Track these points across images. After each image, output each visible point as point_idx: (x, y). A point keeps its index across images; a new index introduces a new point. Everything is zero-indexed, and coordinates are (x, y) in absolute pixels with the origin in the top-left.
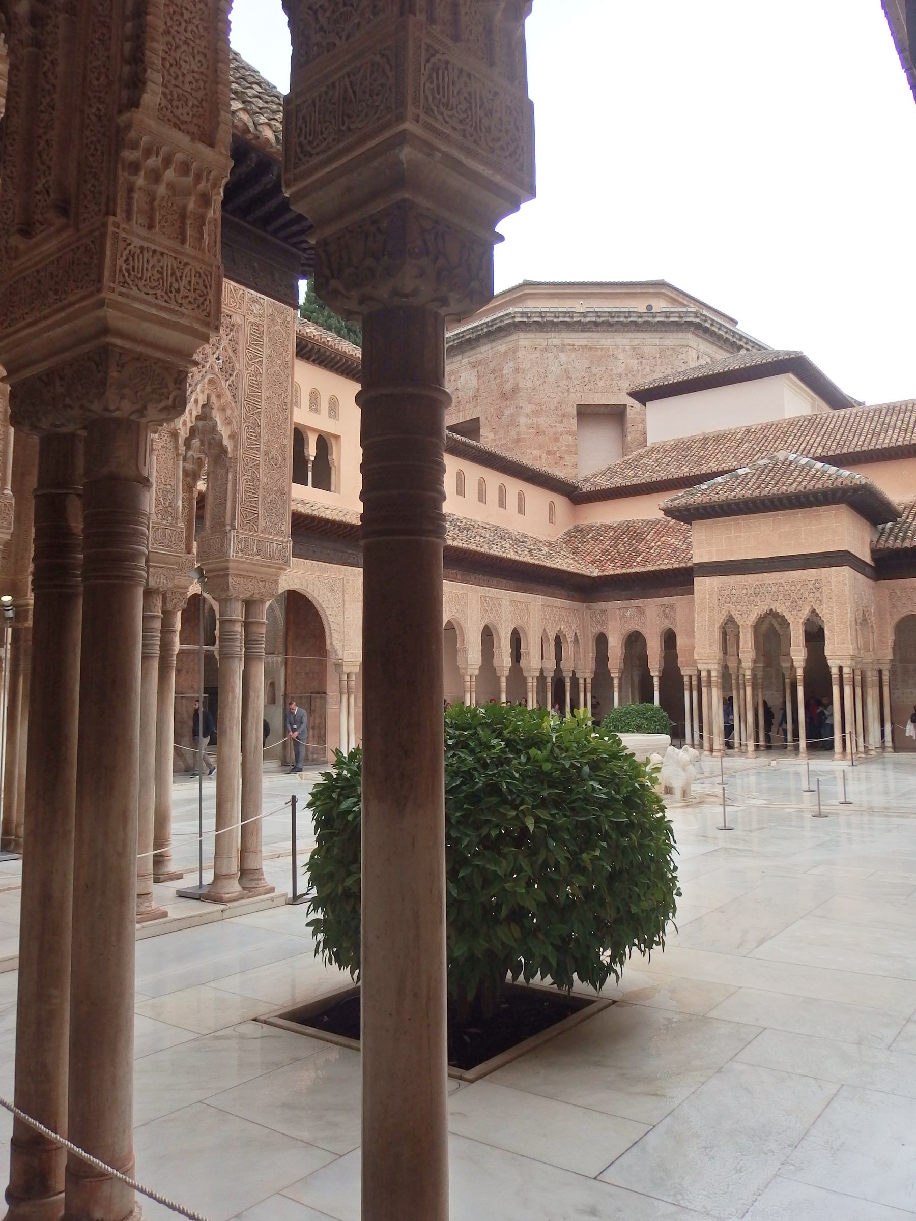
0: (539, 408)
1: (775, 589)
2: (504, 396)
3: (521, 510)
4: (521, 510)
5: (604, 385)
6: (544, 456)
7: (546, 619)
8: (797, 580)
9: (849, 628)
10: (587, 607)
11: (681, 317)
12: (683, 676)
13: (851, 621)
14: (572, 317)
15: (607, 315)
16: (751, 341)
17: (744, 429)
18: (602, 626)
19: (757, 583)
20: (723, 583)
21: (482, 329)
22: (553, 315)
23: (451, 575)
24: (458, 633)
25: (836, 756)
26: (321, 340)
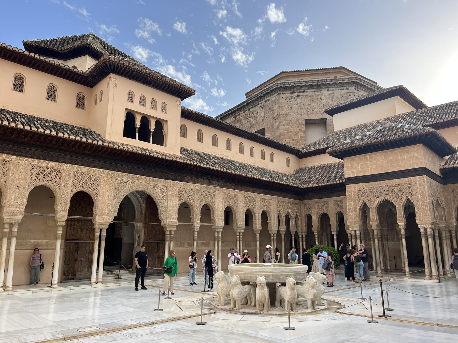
1: (387, 189)
2: (274, 118)
3: (272, 160)
4: (272, 160)
5: (316, 111)
6: (291, 141)
7: (280, 207)
8: (398, 184)
9: (429, 208)
10: (302, 202)
11: (349, 80)
13: (429, 204)
14: (302, 83)
15: (317, 81)
17: (376, 122)
18: (309, 211)
19: (377, 186)
21: (265, 92)
22: (294, 83)
23: (228, 186)
24: (233, 213)
25: (427, 277)
26: (154, 75)
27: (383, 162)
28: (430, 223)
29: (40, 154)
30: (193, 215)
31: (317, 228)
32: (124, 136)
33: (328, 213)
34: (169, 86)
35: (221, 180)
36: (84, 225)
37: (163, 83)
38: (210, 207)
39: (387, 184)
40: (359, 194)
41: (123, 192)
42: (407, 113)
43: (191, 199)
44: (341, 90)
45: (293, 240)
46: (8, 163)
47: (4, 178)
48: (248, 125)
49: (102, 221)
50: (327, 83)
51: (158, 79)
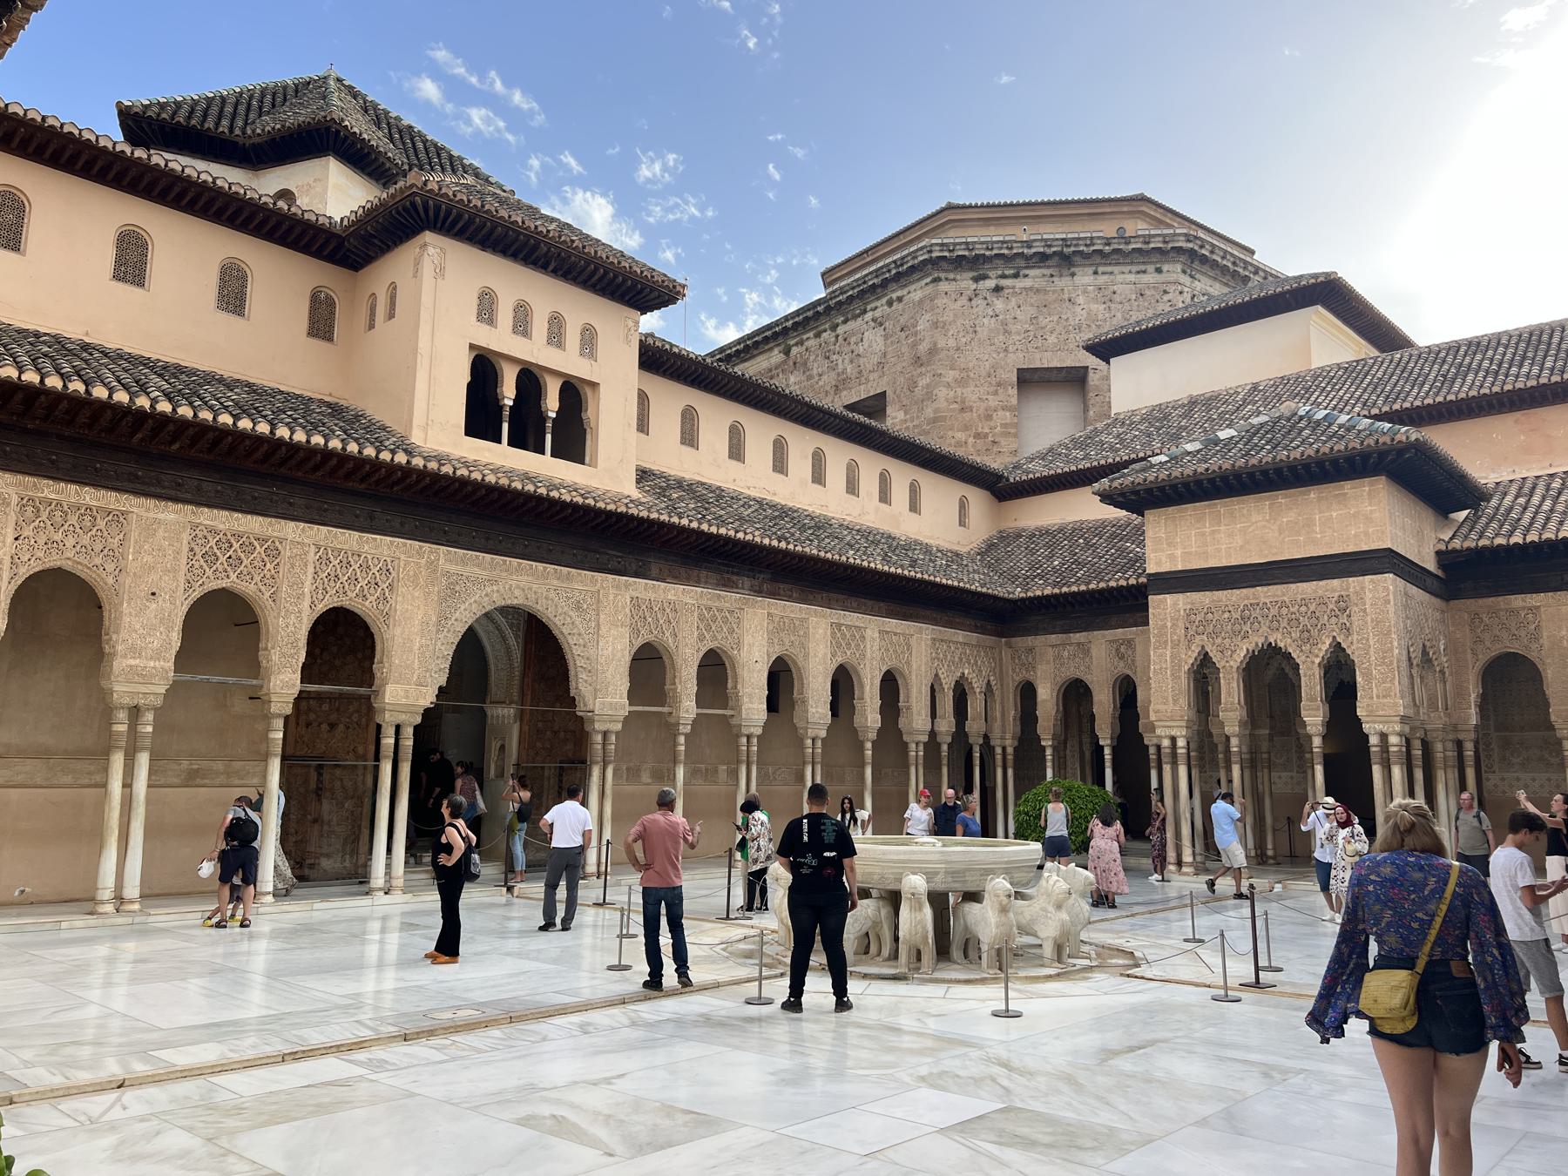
0: (964, 374)
1: (1274, 611)
2: (918, 361)
3: (914, 507)
4: (914, 507)
5: (1056, 341)
6: (971, 440)
7: (938, 659)
8: (1309, 596)
10: (1006, 643)
11: (1165, 242)
12: (1147, 747)
13: (1398, 662)
14: (1011, 248)
15: (1061, 243)
16: (1272, 275)
17: (1248, 387)
18: (1027, 670)
19: (1246, 602)
20: (1192, 604)
21: (889, 271)
22: (984, 246)
23: (782, 592)
26: (560, 237)
27: (1264, 527)
28: (1398, 718)
29: (218, 491)
30: (675, 684)
31: (1052, 724)
32: (468, 433)
33: (1087, 679)
34: (606, 273)
35: (760, 572)
36: (338, 710)
37: (588, 262)
38: (724, 658)
39: (1277, 596)
40: (1187, 625)
41: (465, 610)
42: (1347, 363)
43: (667, 634)
44: (1138, 272)
45: (977, 762)
46: (121, 519)
47: (110, 567)
48: (829, 379)
49: (404, 701)
50: (1092, 248)
51: (573, 249)
